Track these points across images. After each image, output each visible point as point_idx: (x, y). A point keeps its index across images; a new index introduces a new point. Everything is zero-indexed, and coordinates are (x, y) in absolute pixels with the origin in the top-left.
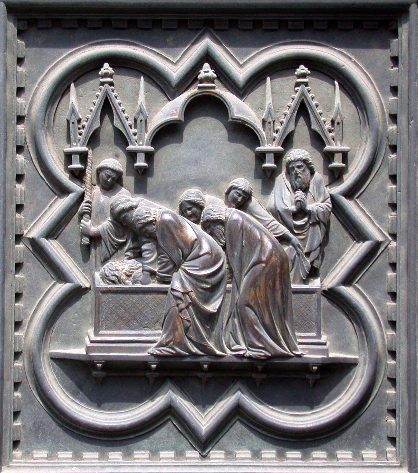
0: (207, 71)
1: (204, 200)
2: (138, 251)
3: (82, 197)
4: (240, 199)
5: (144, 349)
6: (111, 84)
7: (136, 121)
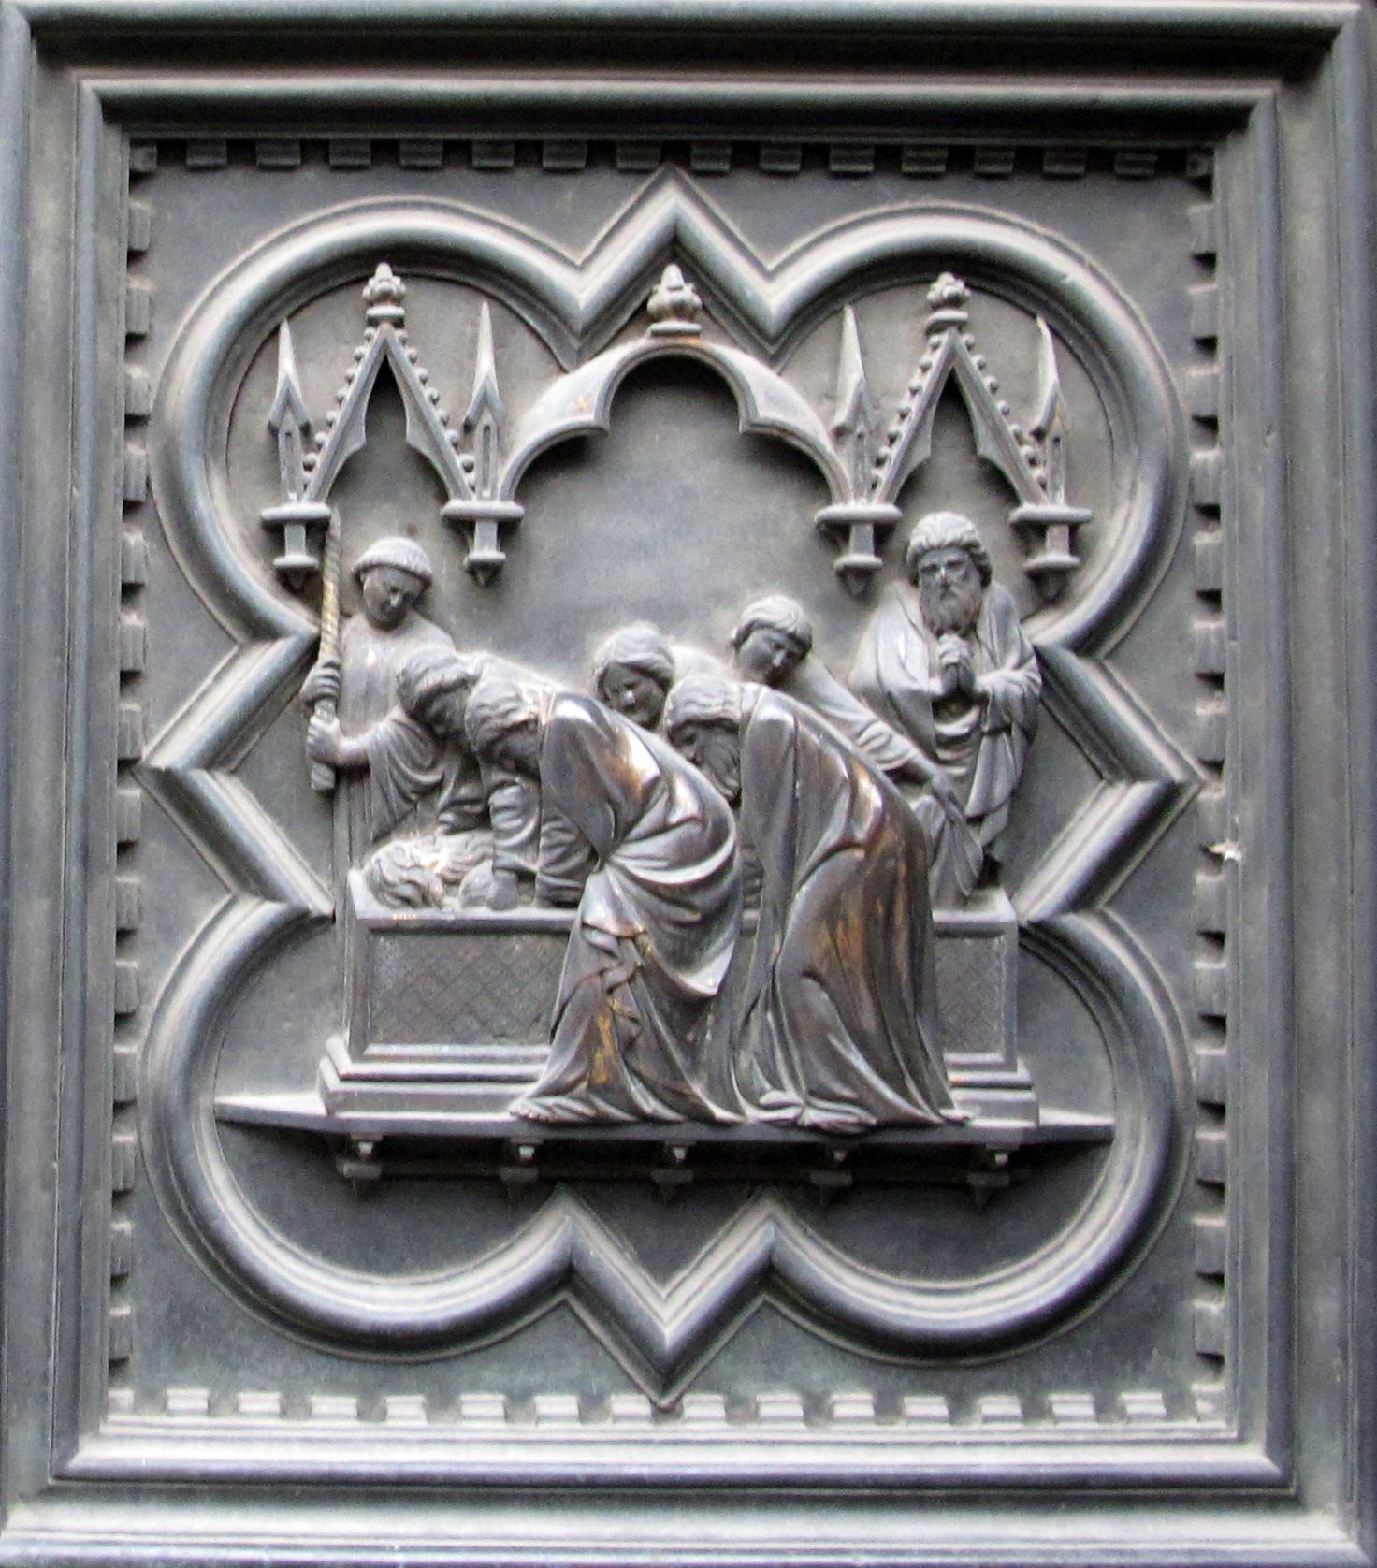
0: (672, 286)
1: (671, 660)
2: (478, 808)
3: (311, 651)
4: (778, 659)
5: (496, 1102)
6: (398, 323)
7: (468, 428)
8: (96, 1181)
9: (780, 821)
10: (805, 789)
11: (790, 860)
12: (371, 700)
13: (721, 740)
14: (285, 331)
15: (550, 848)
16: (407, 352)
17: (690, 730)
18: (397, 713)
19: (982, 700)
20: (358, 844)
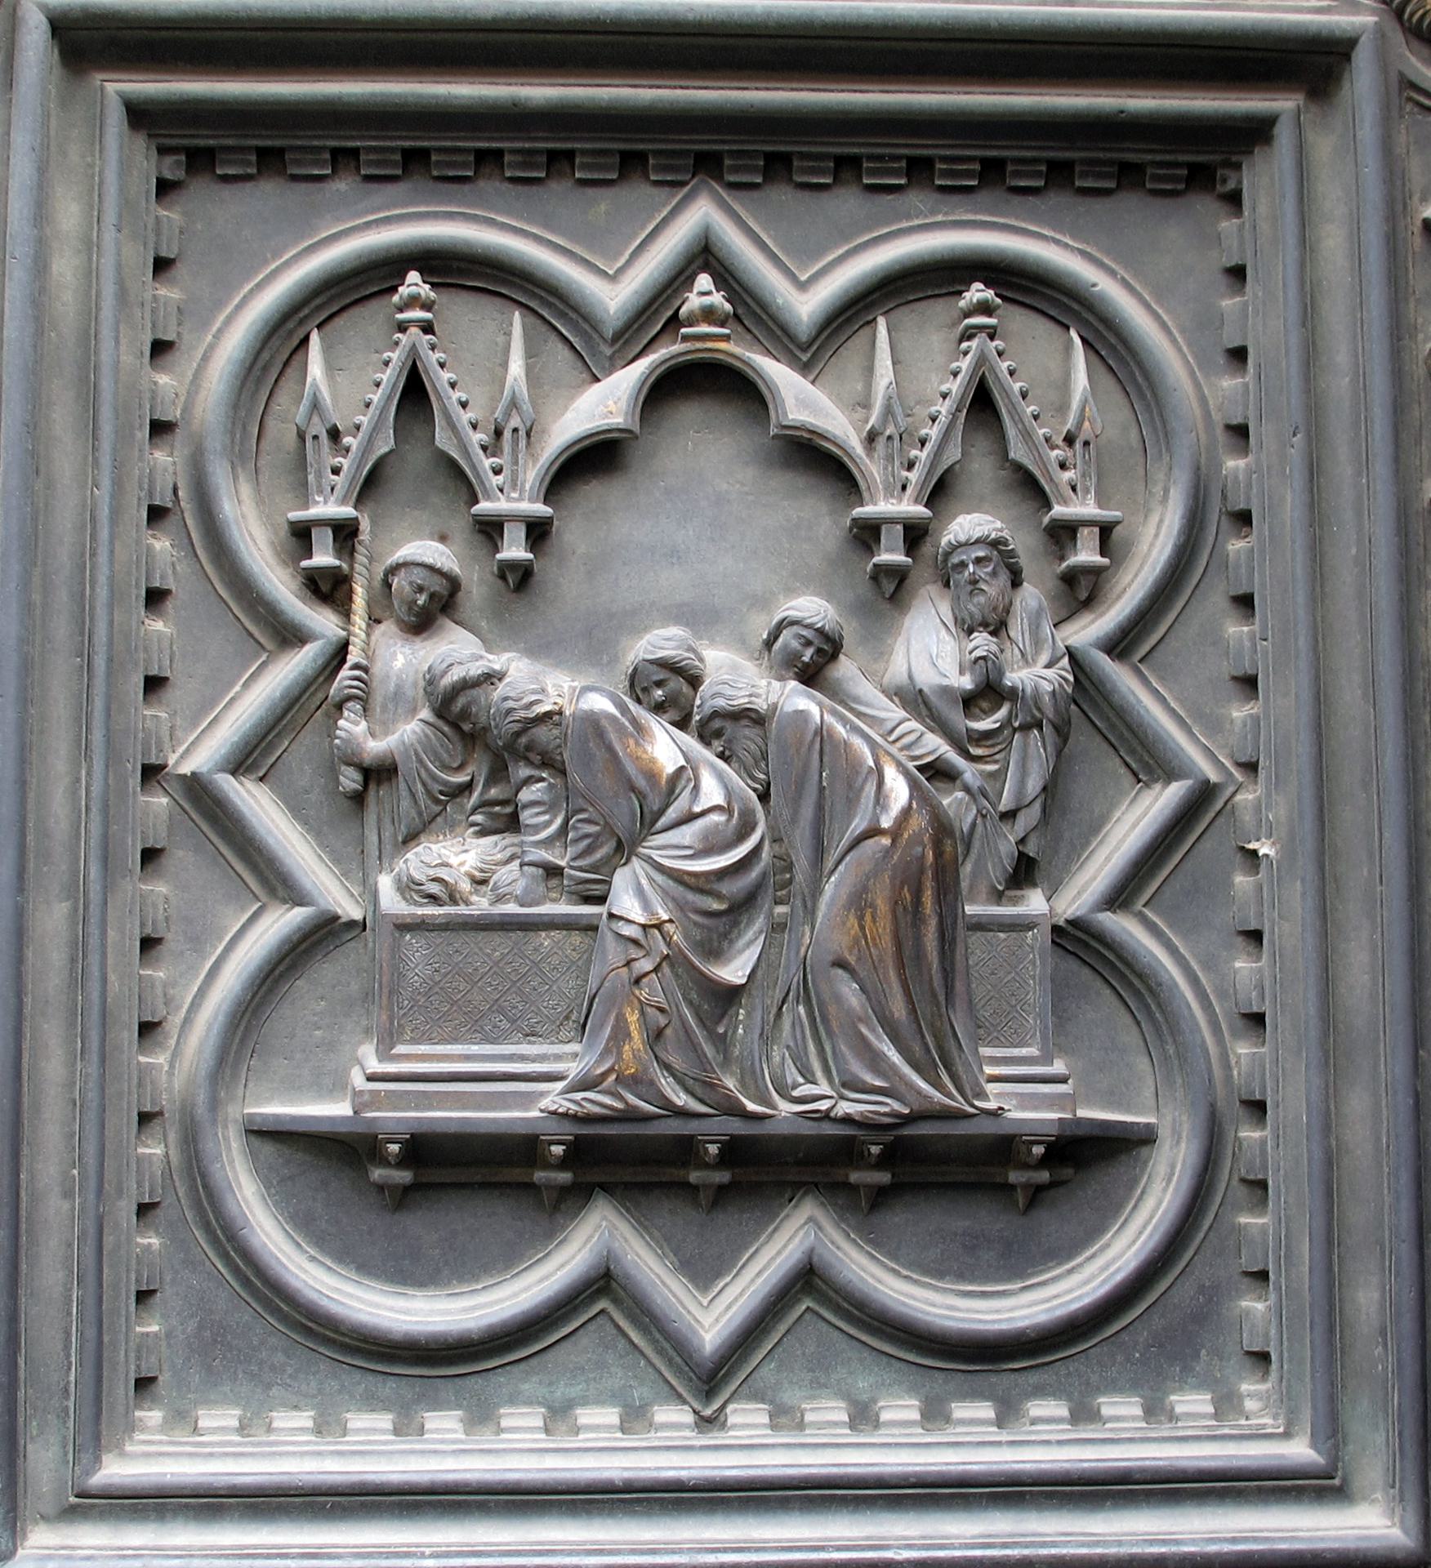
0: (703, 292)
1: (701, 660)
2: (509, 810)
3: (342, 650)
4: (808, 655)
5: (528, 1099)
6: (428, 328)
7: (498, 433)
8: (120, 1192)
9: (807, 812)
10: (831, 776)
11: (819, 851)
12: (400, 704)
13: (747, 737)
14: (315, 338)
15: (576, 841)
16: (435, 356)
17: (717, 724)
18: (425, 713)
19: (1012, 695)
20: (388, 847)
